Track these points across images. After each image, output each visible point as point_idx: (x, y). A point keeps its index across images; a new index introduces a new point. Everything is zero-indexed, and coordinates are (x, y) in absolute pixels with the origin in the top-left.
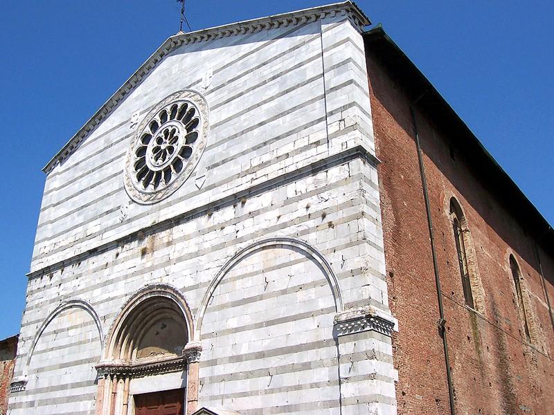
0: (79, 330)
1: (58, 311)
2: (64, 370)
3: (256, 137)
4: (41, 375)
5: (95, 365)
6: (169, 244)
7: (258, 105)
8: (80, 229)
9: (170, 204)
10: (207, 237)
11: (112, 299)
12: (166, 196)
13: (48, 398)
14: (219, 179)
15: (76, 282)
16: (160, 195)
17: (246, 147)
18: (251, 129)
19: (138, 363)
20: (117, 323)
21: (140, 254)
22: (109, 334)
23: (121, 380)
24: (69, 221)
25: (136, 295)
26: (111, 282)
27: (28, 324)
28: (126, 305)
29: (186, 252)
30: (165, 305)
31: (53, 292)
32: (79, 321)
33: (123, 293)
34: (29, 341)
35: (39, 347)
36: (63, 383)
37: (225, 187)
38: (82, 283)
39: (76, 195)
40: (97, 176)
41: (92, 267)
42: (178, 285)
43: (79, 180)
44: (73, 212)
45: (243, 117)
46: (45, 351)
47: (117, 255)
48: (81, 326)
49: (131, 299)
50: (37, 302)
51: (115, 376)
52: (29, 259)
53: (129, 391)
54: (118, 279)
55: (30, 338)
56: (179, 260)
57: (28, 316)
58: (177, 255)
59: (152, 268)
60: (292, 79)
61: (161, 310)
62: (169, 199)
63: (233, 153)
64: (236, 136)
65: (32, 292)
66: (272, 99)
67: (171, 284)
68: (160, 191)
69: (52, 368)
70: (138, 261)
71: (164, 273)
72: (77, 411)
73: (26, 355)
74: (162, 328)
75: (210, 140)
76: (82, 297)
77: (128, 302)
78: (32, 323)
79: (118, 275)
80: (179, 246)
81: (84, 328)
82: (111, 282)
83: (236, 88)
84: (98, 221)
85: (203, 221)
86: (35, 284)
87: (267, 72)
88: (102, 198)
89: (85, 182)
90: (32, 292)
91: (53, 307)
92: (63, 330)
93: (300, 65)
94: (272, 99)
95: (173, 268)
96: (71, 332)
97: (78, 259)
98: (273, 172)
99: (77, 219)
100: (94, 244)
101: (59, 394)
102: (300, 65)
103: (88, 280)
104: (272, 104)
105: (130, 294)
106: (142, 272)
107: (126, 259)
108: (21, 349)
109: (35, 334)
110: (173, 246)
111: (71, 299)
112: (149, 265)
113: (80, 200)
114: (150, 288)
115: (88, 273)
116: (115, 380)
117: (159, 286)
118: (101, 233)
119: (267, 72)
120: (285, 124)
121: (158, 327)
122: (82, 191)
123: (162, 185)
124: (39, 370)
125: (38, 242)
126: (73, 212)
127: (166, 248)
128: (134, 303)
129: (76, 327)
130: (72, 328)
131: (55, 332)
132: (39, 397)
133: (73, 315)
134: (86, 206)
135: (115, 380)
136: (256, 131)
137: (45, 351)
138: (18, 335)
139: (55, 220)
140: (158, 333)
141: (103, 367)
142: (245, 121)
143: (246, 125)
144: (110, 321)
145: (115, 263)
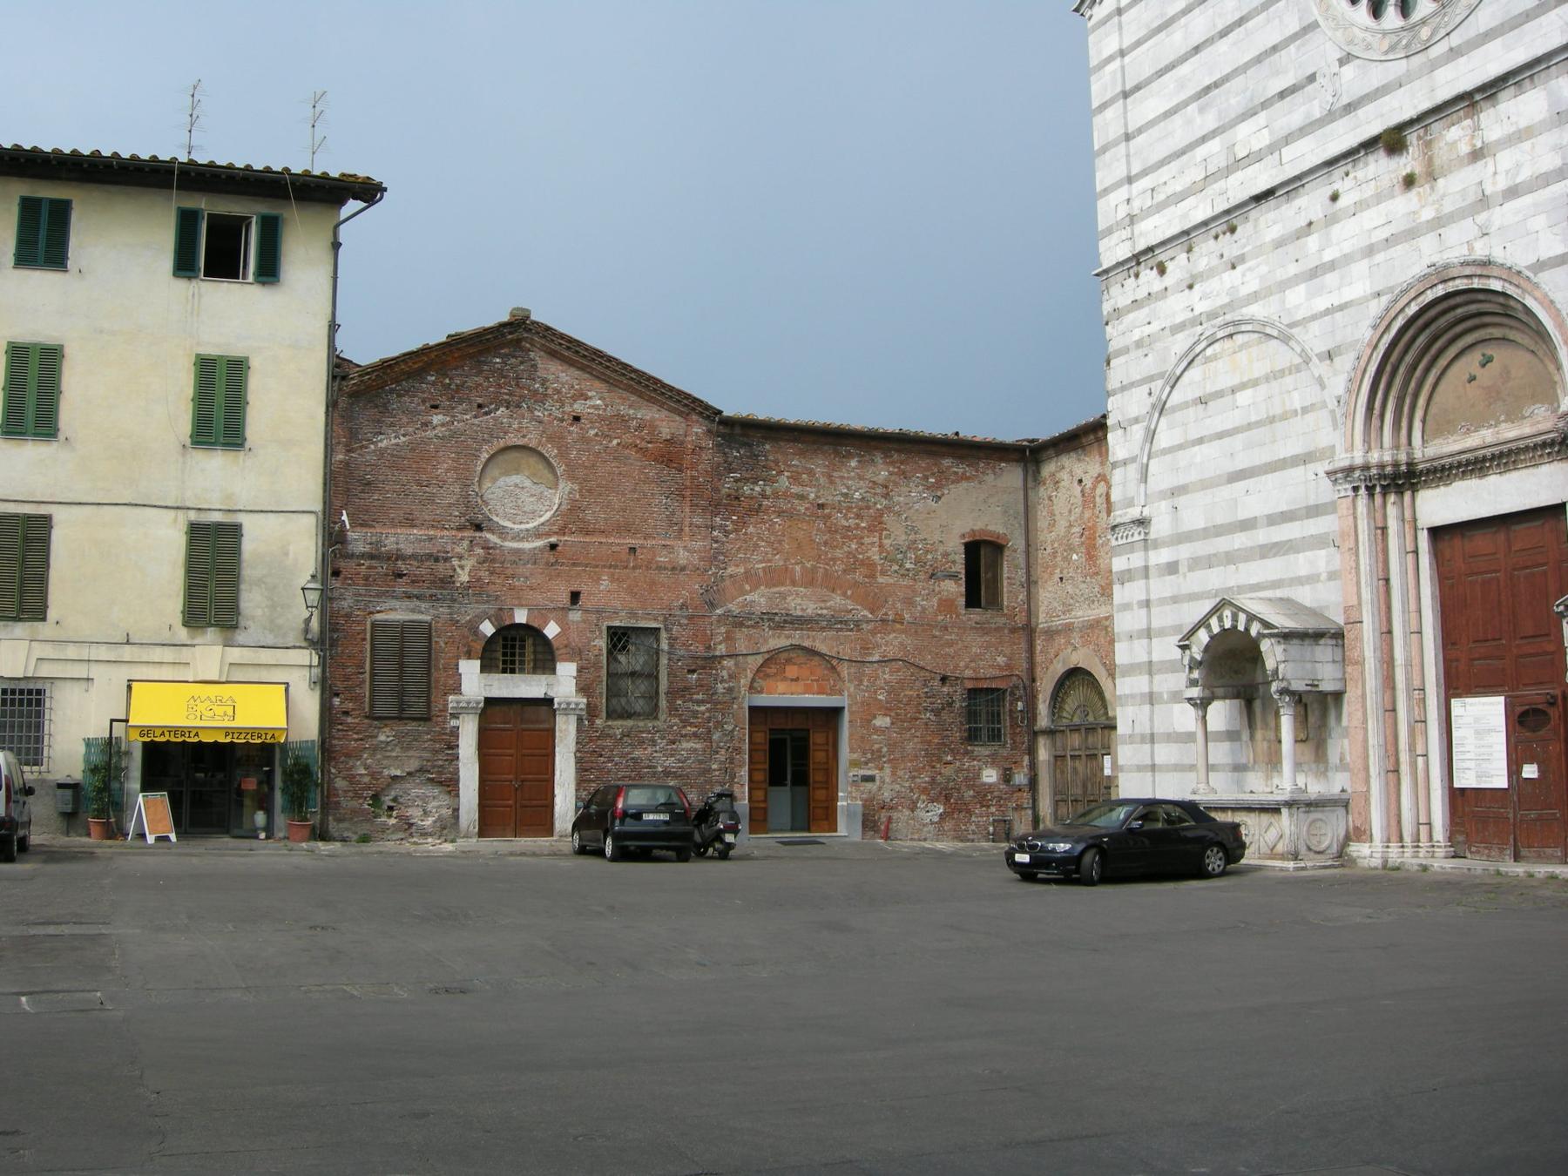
0: (1263, 389)
1: (1198, 350)
2: (1241, 485)
4: (1181, 501)
5: (1322, 467)
6: (1477, 155)
8: (1214, 146)
9: (1454, 53)
11: (1342, 308)
12: (1443, 32)
13: (1212, 552)
15: (1231, 278)
16: (1425, 33)
19: (1431, 451)
20: (1363, 363)
21: (1398, 188)
22: (1349, 391)
23: (1392, 498)
24: (1179, 132)
25: (1404, 292)
26: (1332, 266)
27: (1124, 388)
28: (1382, 318)
29: (1524, 175)
30: (1533, 325)
31: (1177, 307)
32: (1259, 370)
33: (1369, 291)
34: (1136, 427)
35: (1164, 439)
36: (1243, 514)
38: (1246, 280)
39: (1183, 59)
42: (1519, 257)
43: (1183, 20)
44: (1185, 104)
46: (1181, 447)
47: (1334, 198)
48: (1267, 379)
49: (1396, 301)
50: (1137, 335)
51: (1378, 489)
52: (1092, 236)
53: (1415, 520)
54: (1347, 259)
55: (1136, 420)
56: (1513, 192)
57: (1119, 372)
58: (1502, 183)
59: (1439, 223)
61: (1476, 321)
62: (1455, 40)
65: (1118, 313)
67: (1498, 255)
68: (1424, 22)
69: (1206, 485)
70: (1403, 206)
71: (1476, 231)
72: (1292, 575)
73: (1133, 459)
74: (1483, 366)
76: (1256, 310)
77: (1388, 310)
78: (1132, 385)
79: (1347, 247)
80: (1505, 159)
81: (1274, 384)
82: (1332, 266)
84: (1262, 118)
86: (1120, 294)
88: (1258, 60)
90: (1118, 313)
91: (1181, 343)
92: (1219, 394)
95: (1500, 216)
96: (1243, 398)
97: (1228, 220)
99: (1198, 120)
101: (1240, 541)
103: (1264, 269)
105: (1390, 289)
106: (1411, 234)
107: (1360, 206)
108: (1119, 444)
109: (1148, 408)
110: (1490, 160)
111: (1229, 318)
112: (1427, 214)
113: (1196, 73)
114: (1441, 274)
115: (1259, 251)
116: (1378, 499)
117: (1465, 264)
118: (1274, 148)
121: (1475, 357)
122: (1197, 49)
124: (1175, 492)
125: (1106, 191)
126: (1185, 104)
127: (1470, 168)
128: (1402, 310)
129: (1254, 383)
130: (1243, 386)
131: (1202, 401)
132: (1184, 552)
133: (1242, 356)
134: (1216, 85)
135: (1378, 499)
137: (1181, 447)
138: (1104, 417)
139: (1140, 131)
140: (1472, 379)
141: (1349, 471)
144: (1345, 363)
145: (1331, 220)
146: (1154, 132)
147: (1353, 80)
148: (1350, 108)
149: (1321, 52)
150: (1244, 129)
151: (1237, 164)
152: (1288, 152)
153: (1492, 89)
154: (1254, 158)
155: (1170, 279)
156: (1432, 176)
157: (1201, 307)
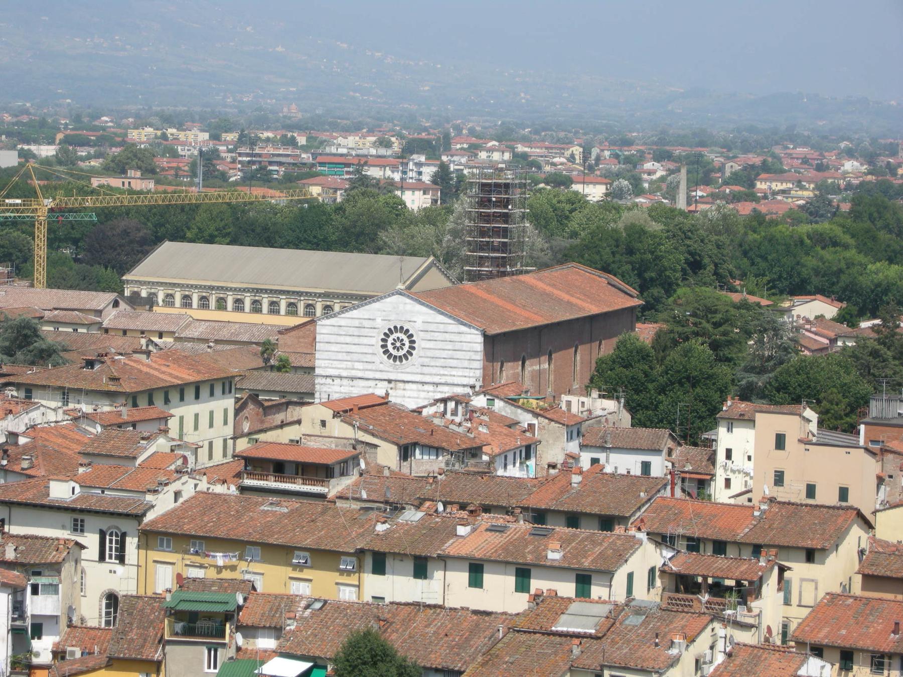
3: (440, 362)
6: (404, 389)
7: (443, 350)
8: (349, 363)
9: (402, 372)
10: (421, 393)
14: (425, 372)
15: (351, 389)
17: (438, 365)
18: (440, 358)
24: (340, 356)
37: (428, 376)
40: (356, 340)
41: (363, 385)
45: (437, 351)
56: (409, 397)
60: (458, 346)
63: (432, 364)
64: (433, 358)
66: (449, 350)
75: (422, 354)
83: (433, 336)
85: (420, 386)
87: (448, 337)
88: (362, 353)
89: (348, 339)
93: (461, 342)
94: (449, 350)
97: (352, 379)
98: (450, 380)
100: (360, 374)
102: (461, 342)
104: (450, 352)
119: (448, 337)
120: (453, 363)
123: (398, 362)
136: (443, 360)
142: (438, 354)
143: (438, 355)
146: (334, 353)
147: (382, 367)
148: (381, 371)
149: (376, 359)
150: (356, 364)
151: (353, 369)
152: (366, 372)
153: (408, 382)
154: (358, 369)
155: (334, 383)
156: (396, 389)
157: (343, 391)
